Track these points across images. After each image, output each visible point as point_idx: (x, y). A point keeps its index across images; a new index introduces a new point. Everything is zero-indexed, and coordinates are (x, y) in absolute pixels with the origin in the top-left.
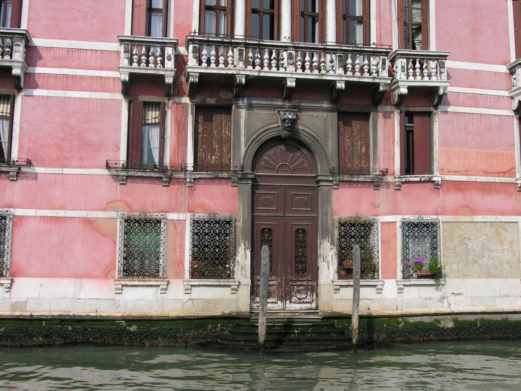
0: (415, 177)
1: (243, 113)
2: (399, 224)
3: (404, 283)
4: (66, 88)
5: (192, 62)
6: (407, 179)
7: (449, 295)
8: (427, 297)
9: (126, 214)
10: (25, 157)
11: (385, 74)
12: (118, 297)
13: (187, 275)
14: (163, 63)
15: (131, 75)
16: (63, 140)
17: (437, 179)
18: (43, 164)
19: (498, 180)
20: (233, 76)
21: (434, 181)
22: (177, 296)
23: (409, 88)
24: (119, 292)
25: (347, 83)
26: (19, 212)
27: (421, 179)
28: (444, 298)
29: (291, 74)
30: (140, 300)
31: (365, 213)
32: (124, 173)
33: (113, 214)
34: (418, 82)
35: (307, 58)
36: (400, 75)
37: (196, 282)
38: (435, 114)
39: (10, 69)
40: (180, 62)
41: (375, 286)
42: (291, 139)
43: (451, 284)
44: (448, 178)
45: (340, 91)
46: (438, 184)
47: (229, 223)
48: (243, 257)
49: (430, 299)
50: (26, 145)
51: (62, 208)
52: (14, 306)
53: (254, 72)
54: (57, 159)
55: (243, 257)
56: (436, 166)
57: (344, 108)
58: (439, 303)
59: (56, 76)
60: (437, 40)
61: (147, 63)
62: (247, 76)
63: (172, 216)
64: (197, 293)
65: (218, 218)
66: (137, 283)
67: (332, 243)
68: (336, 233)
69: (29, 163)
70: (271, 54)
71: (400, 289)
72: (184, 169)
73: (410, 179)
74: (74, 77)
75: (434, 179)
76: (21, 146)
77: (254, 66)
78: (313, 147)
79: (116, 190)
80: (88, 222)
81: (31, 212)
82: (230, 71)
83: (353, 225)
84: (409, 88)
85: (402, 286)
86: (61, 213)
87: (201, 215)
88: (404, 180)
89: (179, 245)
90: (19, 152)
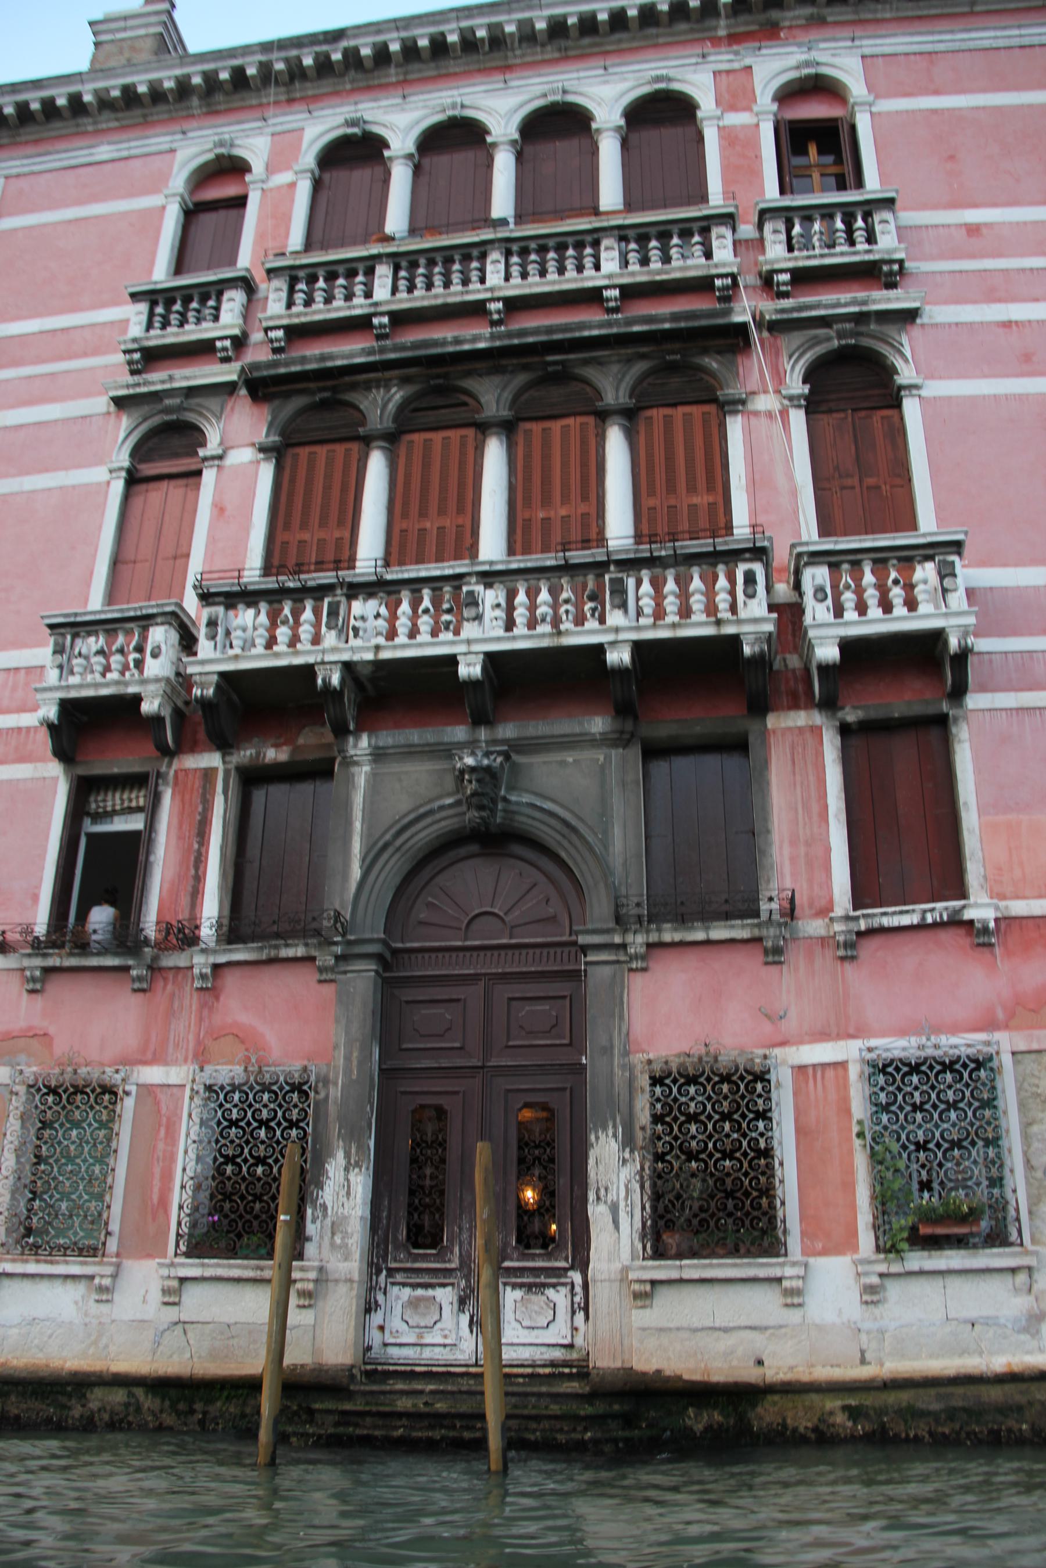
0: (901, 912)
1: (362, 775)
2: (854, 1071)
3: (882, 1268)
6: (876, 923)
8: (973, 1314)
9: (31, 1071)
11: (757, 608)
14: (139, 664)
17: (980, 909)
20: (309, 670)
21: (971, 922)
25: (638, 647)
27: (923, 918)
29: (473, 643)
31: (734, 1039)
32: (38, 962)
34: (875, 624)
35: (521, 598)
36: (816, 612)
37: (192, 1268)
38: (956, 719)
41: (779, 1280)
42: (489, 833)
44: (1019, 908)
45: (620, 672)
46: (985, 930)
47: (298, 1088)
49: (989, 1322)
53: (362, 650)
55: (346, 1192)
56: (974, 872)
58: (1024, 1337)
62: (348, 667)
63: (152, 1074)
64: (197, 1302)
66: (32, 1268)
67: (628, 1142)
70: (415, 604)
71: (870, 1289)
73: (886, 922)
75: (968, 915)
83: (692, 1080)
85: (875, 1280)
88: (863, 925)
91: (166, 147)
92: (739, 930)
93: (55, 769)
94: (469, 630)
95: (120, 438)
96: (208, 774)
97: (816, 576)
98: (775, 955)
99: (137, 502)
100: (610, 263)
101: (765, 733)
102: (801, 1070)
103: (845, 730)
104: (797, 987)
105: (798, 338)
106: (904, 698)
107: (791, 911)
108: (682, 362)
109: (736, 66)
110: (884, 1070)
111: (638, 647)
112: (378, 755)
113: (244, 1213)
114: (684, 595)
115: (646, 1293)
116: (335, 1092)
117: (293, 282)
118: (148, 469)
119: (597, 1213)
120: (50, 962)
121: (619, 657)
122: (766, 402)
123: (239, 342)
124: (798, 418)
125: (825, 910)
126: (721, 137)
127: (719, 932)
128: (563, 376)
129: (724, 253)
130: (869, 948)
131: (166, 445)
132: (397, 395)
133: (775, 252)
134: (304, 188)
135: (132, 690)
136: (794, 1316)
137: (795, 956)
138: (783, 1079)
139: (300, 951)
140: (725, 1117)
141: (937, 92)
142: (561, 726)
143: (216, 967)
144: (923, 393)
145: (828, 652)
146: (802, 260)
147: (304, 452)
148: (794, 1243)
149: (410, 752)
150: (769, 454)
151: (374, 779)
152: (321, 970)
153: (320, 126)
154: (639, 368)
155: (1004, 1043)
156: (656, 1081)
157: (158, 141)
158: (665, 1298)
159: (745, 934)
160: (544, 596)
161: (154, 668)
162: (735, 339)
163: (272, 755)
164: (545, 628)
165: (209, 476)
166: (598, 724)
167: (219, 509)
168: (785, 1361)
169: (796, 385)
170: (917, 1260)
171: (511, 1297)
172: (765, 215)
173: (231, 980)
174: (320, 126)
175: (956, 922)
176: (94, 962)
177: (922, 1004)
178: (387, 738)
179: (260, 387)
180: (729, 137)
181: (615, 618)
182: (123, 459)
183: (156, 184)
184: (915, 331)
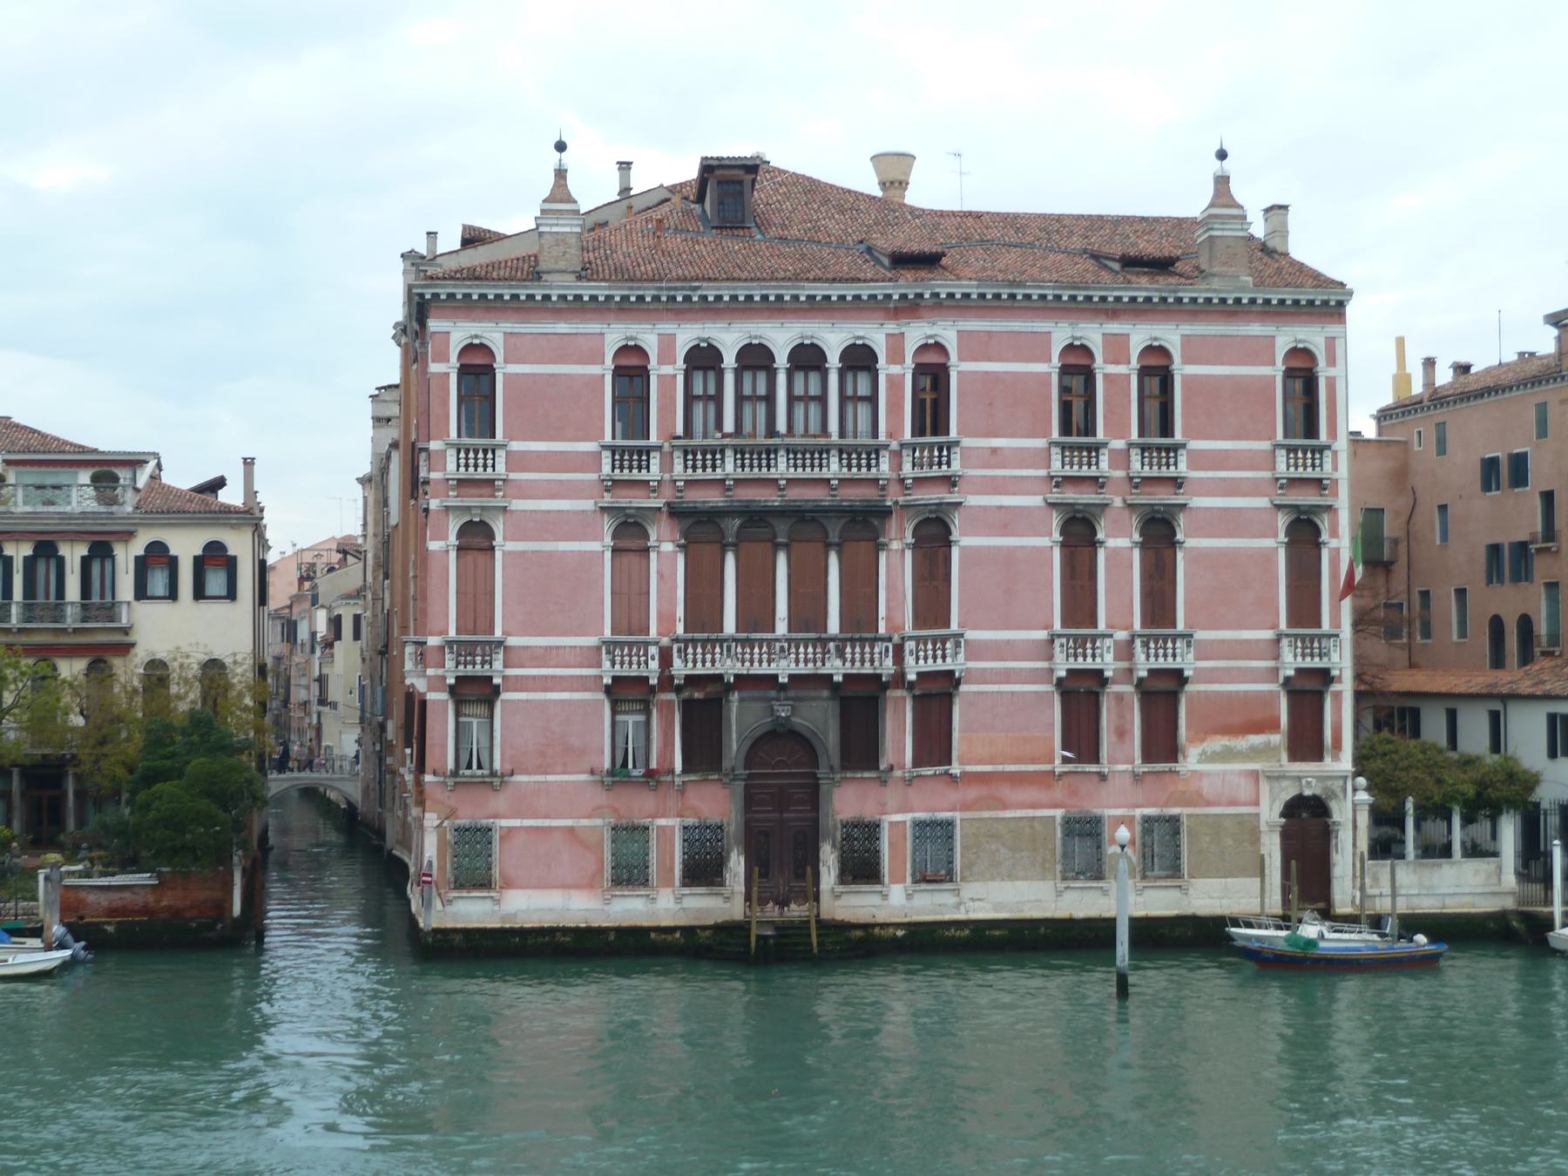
4: (545, 690)
5: (677, 662)
10: (508, 767)
11: (889, 662)
13: (677, 883)
14: (646, 663)
15: (614, 678)
17: (956, 769)
18: (526, 772)
19: (1031, 768)
22: (666, 905)
23: (919, 674)
24: (607, 902)
25: (845, 676)
26: (505, 823)
28: (960, 904)
29: (784, 669)
30: (629, 909)
31: (868, 813)
33: (598, 822)
36: (910, 661)
37: (687, 891)
39: (491, 678)
40: (665, 658)
44: (969, 768)
45: (838, 683)
47: (720, 827)
48: (737, 864)
51: (547, 817)
52: (503, 919)
55: (737, 864)
59: (534, 677)
61: (630, 663)
63: (662, 822)
65: (708, 822)
67: (834, 846)
68: (838, 834)
69: (512, 774)
72: (672, 771)
74: (553, 677)
76: (503, 755)
77: (743, 662)
78: (813, 741)
79: (602, 798)
80: (571, 830)
81: (516, 823)
82: (718, 669)
84: (919, 674)
86: (547, 823)
87: (690, 821)
89: (667, 853)
90: (502, 760)
92: (873, 775)
95: (607, 525)
96: (671, 702)
98: (884, 783)
100: (835, 466)
102: (891, 823)
103: (914, 697)
104: (892, 795)
105: (911, 512)
106: (936, 695)
107: (891, 768)
108: (862, 523)
110: (919, 825)
111: (845, 676)
112: (741, 700)
113: (702, 870)
114: (862, 654)
115: (838, 897)
116: (732, 828)
117: (686, 453)
119: (823, 870)
121: (838, 678)
122: (895, 545)
124: (908, 554)
125: (903, 767)
127: (866, 775)
129: (885, 465)
130: (915, 782)
131: (630, 532)
132: (737, 522)
133: (907, 468)
134: (680, 379)
137: (890, 783)
142: (812, 693)
145: (912, 677)
148: (886, 880)
149: (754, 699)
150: (896, 568)
151: (739, 708)
153: (687, 335)
154: (843, 521)
155: (957, 816)
156: (844, 826)
157: (593, 327)
160: (810, 650)
162: (886, 513)
163: (697, 695)
164: (810, 665)
165: (653, 556)
166: (825, 693)
167: (661, 575)
170: (924, 886)
172: (902, 445)
173: (689, 787)
174: (687, 335)
175: (946, 773)
178: (745, 694)
179: (676, 512)
180: (889, 377)
182: (608, 541)
184: (961, 510)
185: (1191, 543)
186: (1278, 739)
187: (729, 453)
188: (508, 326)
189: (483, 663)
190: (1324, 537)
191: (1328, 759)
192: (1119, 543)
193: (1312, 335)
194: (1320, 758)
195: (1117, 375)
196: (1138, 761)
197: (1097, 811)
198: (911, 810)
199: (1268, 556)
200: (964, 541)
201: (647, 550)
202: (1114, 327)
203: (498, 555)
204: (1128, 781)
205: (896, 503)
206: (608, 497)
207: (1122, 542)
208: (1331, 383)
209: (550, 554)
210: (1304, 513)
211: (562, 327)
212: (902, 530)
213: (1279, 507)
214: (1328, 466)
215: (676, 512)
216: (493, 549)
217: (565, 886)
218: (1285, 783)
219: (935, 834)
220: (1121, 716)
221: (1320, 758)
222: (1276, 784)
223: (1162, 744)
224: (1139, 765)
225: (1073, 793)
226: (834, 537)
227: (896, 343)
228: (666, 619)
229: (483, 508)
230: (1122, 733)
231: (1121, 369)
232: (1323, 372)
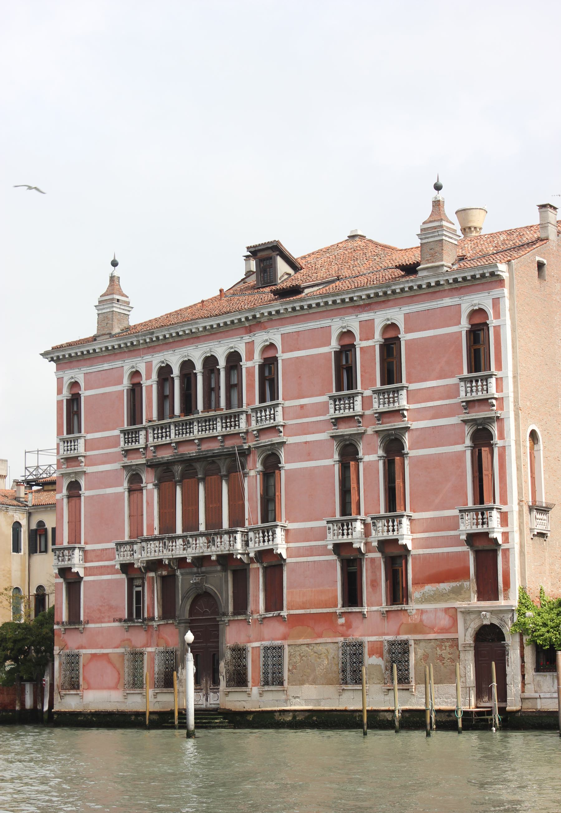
4: (101, 574)
7: (291, 698)
10: (87, 619)
12: (126, 701)
16: (101, 606)
17: (284, 613)
18: (94, 622)
25: (218, 556)
29: (190, 554)
32: (126, 625)
43: (292, 690)
49: (279, 700)
50: (86, 611)
51: (102, 648)
54: (99, 618)
57: (233, 568)
60: (286, 509)
66: (132, 692)
69: (88, 622)
71: (260, 694)
72: (153, 619)
74: (105, 566)
75: (281, 614)
76: (84, 612)
89: (151, 667)
91: (120, 365)
93: (124, 576)
94: (189, 550)
97: (251, 534)
99: (132, 496)
101: (249, 569)
102: (253, 648)
103: (265, 569)
104: (252, 631)
105: (260, 450)
109: (250, 340)
110: (266, 649)
112: (182, 574)
115: (227, 694)
118: (134, 486)
119: (221, 677)
120: (129, 625)
122: (252, 473)
123: (146, 448)
126: (246, 372)
128: (213, 462)
129: (243, 425)
131: (135, 480)
135: (132, 562)
136: (249, 699)
138: (250, 649)
139: (171, 622)
140: (239, 658)
141: (299, 350)
143: (158, 625)
144: (285, 468)
145: (252, 555)
146: (260, 426)
147: (164, 484)
148: (250, 684)
149: (187, 574)
151: (182, 579)
152: (176, 626)
153: (157, 360)
154: (228, 461)
157: (118, 364)
158: (230, 695)
159: (244, 618)
161: (136, 556)
162: (245, 454)
163: (165, 573)
165: (144, 491)
167: (148, 503)
168: (249, 707)
169: (259, 467)
170: (266, 688)
171: (212, 694)
173: (161, 628)
175: (279, 615)
176: (136, 624)
177: (273, 634)
179: (152, 465)
181: (213, 548)
182: (126, 485)
183: (120, 382)
184: (286, 446)
185: (413, 453)
186: (471, 584)
187: (172, 427)
188: (85, 370)
189: (69, 560)
190: (496, 440)
191: (501, 597)
192: (371, 457)
193: (482, 299)
194: (497, 599)
195: (368, 346)
196: (384, 604)
197: (360, 639)
198: (263, 640)
199: (460, 456)
200: (287, 465)
201: (141, 490)
202: (365, 316)
203: (83, 498)
204: (378, 617)
205: (250, 446)
206: (125, 460)
207: (372, 458)
208: (497, 329)
209: (103, 495)
210: (481, 424)
211: (106, 366)
212: (255, 463)
213: (465, 422)
214: (493, 389)
215: (152, 465)
216: (79, 496)
217: (109, 688)
218: (473, 616)
219: (274, 654)
220: (374, 573)
221: (497, 599)
222: (468, 618)
223: (397, 593)
224: (384, 607)
225: (348, 625)
226: (224, 472)
227: (250, 346)
228: (151, 527)
229: (76, 473)
230: (374, 584)
231: (365, 344)
232: (492, 322)
